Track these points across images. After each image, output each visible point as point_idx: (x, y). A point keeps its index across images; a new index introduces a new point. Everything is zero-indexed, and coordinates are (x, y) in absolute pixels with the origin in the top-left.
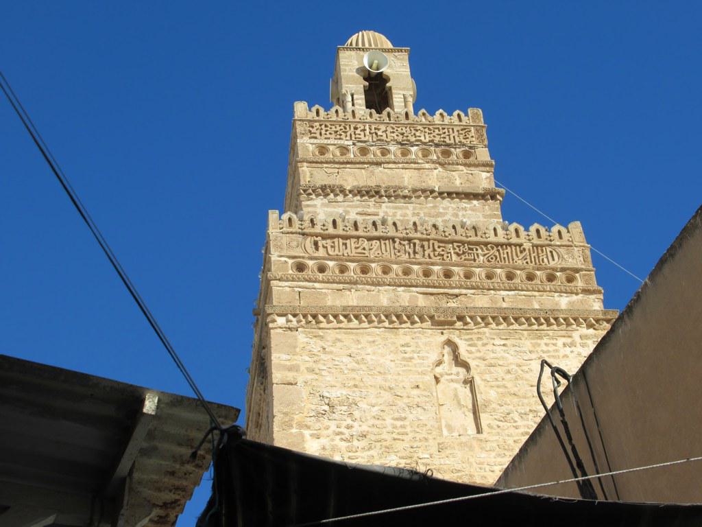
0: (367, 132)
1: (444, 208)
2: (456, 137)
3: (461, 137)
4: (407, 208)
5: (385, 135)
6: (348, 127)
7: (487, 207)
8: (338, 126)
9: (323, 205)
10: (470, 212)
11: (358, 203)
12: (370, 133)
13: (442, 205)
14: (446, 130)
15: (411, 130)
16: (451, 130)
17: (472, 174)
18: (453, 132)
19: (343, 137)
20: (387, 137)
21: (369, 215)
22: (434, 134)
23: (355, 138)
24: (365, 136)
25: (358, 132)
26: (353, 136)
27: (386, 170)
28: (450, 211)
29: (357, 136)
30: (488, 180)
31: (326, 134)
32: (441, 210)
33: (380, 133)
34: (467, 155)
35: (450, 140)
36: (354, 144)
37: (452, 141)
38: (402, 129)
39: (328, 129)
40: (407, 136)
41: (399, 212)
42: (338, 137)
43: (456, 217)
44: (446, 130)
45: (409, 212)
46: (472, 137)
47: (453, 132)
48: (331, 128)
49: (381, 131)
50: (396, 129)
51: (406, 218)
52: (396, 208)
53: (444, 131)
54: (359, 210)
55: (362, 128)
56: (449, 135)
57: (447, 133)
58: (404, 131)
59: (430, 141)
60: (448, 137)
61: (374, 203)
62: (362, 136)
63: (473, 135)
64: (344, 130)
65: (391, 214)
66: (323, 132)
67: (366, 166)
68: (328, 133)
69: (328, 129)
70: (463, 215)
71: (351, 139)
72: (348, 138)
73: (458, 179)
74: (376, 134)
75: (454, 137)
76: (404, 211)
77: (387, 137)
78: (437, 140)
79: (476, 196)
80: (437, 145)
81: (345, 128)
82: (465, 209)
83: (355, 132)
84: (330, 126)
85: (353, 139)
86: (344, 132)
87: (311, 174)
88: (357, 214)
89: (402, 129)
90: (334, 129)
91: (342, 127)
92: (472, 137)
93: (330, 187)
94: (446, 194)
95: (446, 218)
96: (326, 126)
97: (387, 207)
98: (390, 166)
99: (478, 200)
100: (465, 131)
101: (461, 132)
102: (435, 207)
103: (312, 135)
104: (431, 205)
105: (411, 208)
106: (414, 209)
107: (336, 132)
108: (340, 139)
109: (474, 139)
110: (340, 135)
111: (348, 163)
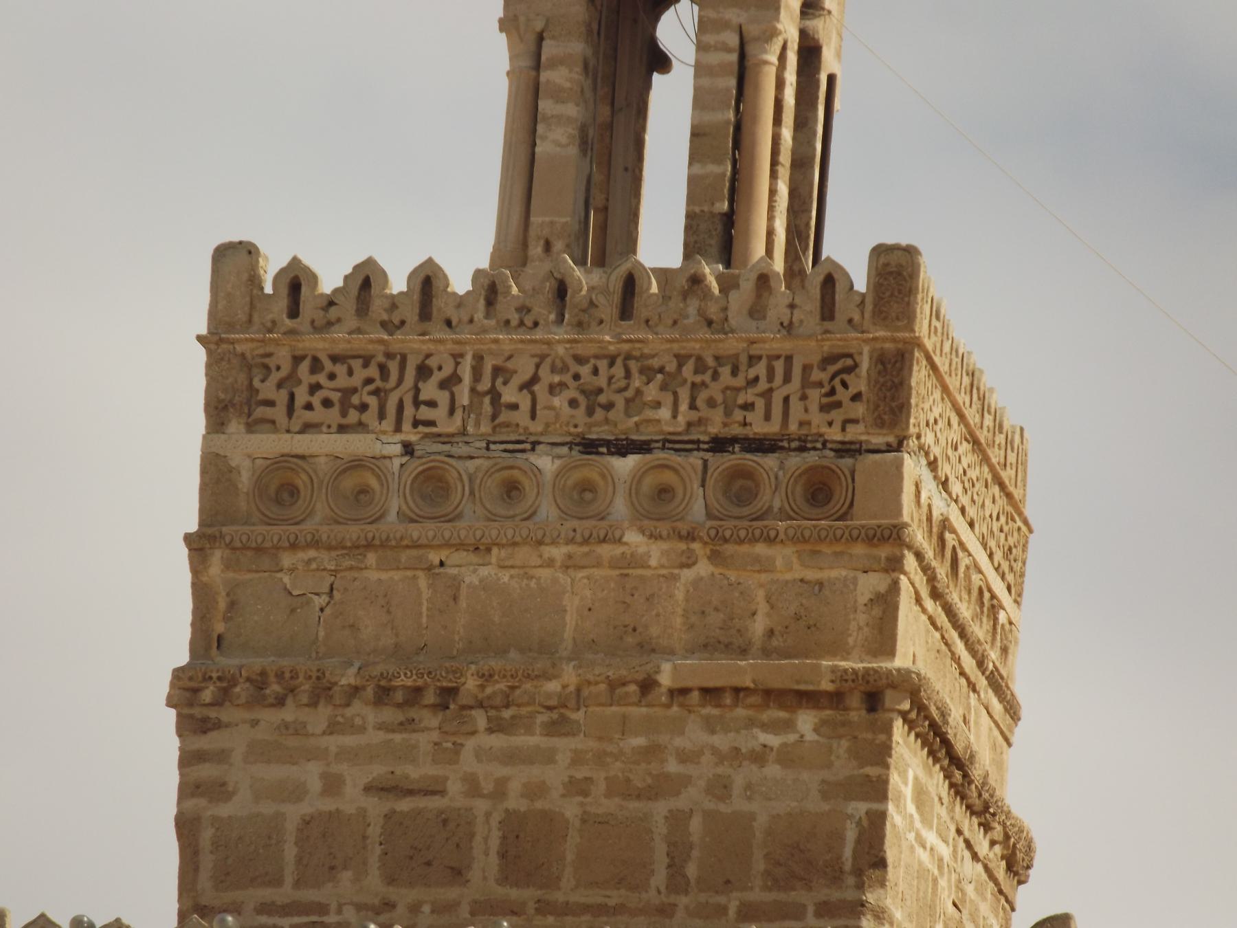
0: (464, 398)
1: (685, 757)
2: (794, 401)
3: (815, 395)
4: (549, 757)
5: (525, 404)
6: (393, 367)
7: (845, 743)
8: (356, 364)
9: (260, 752)
10: (773, 770)
11: (381, 736)
12: (473, 390)
13: (678, 742)
14: (760, 369)
15: (628, 375)
16: (779, 366)
17: (821, 584)
18: (787, 379)
19: (370, 417)
20: (533, 416)
21: (411, 792)
22: (715, 390)
23: (416, 423)
24: (452, 411)
25: (429, 390)
26: (409, 411)
27: (505, 577)
28: (706, 769)
29: (425, 413)
30: (877, 611)
31: (309, 406)
32: (673, 767)
33: (509, 394)
34: (819, 491)
35: (767, 417)
36: (408, 449)
37: (773, 428)
38: (595, 371)
39: (322, 378)
40: (609, 406)
41: (518, 777)
42: (353, 416)
43: (721, 799)
44: (760, 369)
45: (555, 776)
46: (856, 397)
47: (787, 379)
48: (332, 377)
49: (516, 381)
50: (574, 368)
51: (539, 805)
52: (512, 757)
53: (752, 373)
54: (377, 770)
55: (447, 371)
56: (767, 394)
57: (763, 385)
58: (602, 381)
59: (689, 424)
60: (760, 404)
61: (435, 736)
62: (439, 414)
63: (863, 388)
64: (378, 383)
65: (487, 787)
66: (302, 396)
67: (434, 557)
68: (316, 400)
69: (322, 378)
70: (749, 786)
71: (398, 429)
72: (388, 424)
73: (763, 608)
74: (495, 395)
75: (786, 400)
76: (536, 772)
77: (533, 416)
78: (714, 429)
79: (808, 698)
80: (719, 445)
81: (383, 368)
82: (759, 757)
83: (417, 390)
84: (328, 366)
85: (407, 426)
86: (376, 392)
87: (232, 605)
88: (368, 789)
89: (595, 371)
90: (343, 381)
91: (373, 371)
92: (856, 397)
93: (280, 675)
94: (696, 694)
95: (681, 803)
96: (316, 366)
97: (479, 754)
98: (524, 554)
99: (817, 707)
100: (832, 369)
101: (817, 375)
102: (652, 752)
103: (260, 412)
104: (639, 741)
105: (563, 759)
106: (577, 759)
107: (349, 392)
108: (361, 427)
109: (859, 410)
110: (364, 407)
111: (369, 546)
